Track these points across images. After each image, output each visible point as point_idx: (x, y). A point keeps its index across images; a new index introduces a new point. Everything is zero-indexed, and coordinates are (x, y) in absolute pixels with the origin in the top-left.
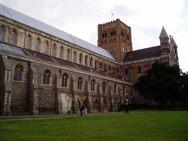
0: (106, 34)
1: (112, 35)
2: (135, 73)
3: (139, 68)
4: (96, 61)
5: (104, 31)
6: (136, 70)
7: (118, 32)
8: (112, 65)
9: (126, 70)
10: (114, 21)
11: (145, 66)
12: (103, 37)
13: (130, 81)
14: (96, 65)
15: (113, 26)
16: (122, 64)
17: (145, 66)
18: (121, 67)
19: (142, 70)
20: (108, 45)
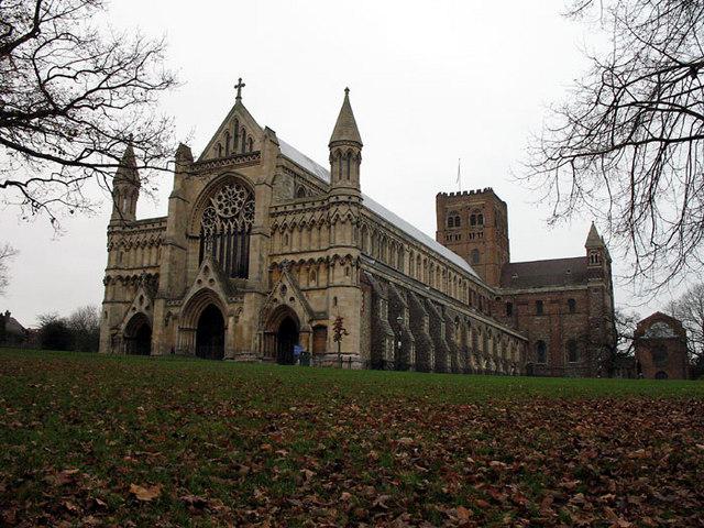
0: (458, 219)
1: (473, 223)
2: (529, 315)
3: (539, 303)
4: (470, 290)
5: (455, 212)
6: (532, 309)
7: (488, 219)
8: (487, 296)
9: (509, 305)
10: (479, 191)
11: (552, 302)
12: (450, 225)
13: (516, 329)
14: (470, 299)
15: (475, 204)
16: (500, 292)
17: (552, 302)
18: (498, 299)
19: (546, 309)
20: (465, 246)
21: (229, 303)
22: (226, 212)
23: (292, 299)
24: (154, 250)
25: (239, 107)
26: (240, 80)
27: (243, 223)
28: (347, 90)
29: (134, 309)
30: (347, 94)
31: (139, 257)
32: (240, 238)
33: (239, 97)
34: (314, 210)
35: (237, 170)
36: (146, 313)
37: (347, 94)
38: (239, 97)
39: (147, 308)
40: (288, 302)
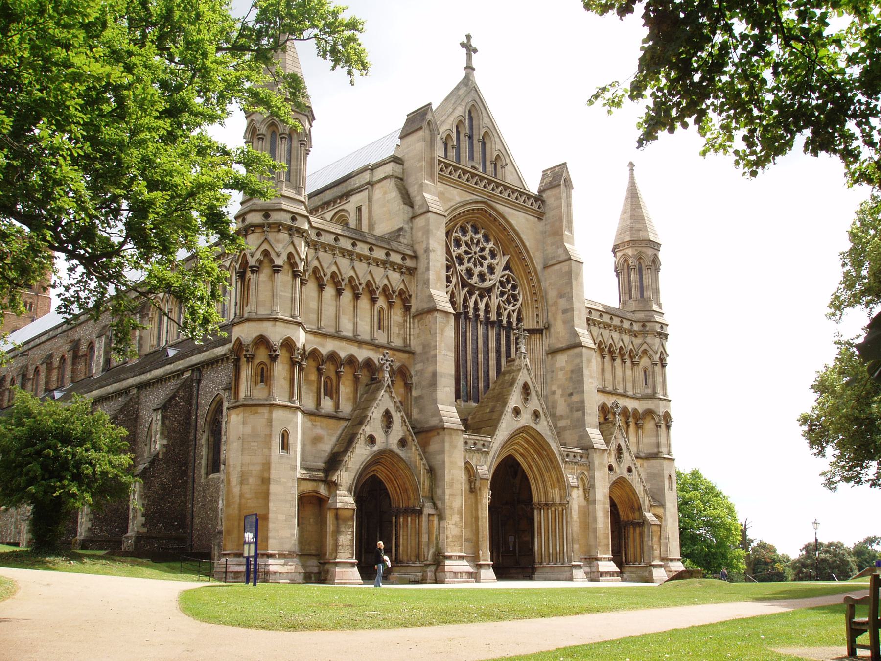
21: (566, 462)
22: (470, 273)
23: (630, 470)
24: (364, 303)
25: (468, 83)
26: (468, 37)
27: (499, 307)
28: (631, 165)
29: (372, 440)
30: (632, 170)
31: (329, 310)
32: (492, 334)
33: (469, 68)
34: (620, 330)
35: (499, 207)
36: (402, 454)
37: (632, 170)
38: (469, 68)
39: (403, 443)
40: (625, 474)
